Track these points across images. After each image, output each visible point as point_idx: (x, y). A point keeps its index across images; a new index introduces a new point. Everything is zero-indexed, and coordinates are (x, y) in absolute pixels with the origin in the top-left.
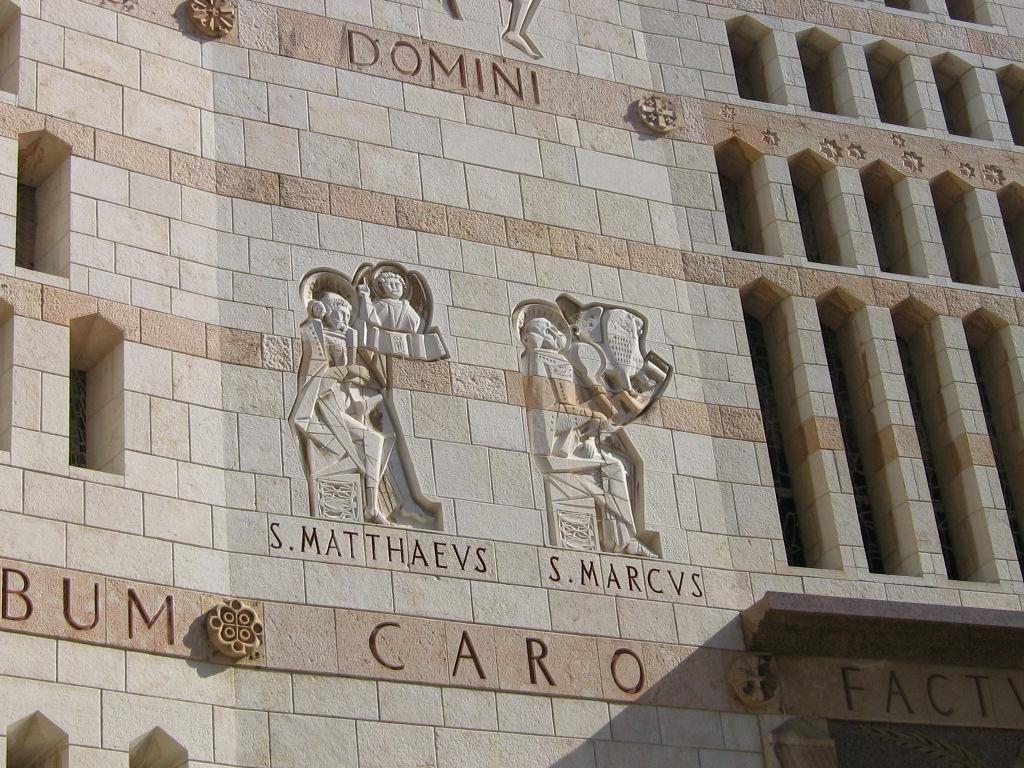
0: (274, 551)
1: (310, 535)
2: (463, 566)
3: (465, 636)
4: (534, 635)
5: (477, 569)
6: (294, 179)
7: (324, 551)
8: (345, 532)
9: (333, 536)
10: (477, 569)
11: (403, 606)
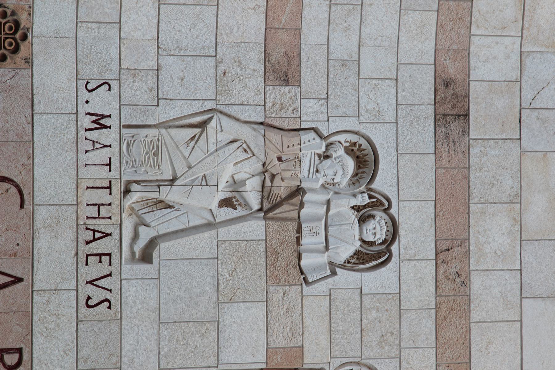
0: (82, 83)
1: (103, 122)
2: (91, 282)
3: (19, 280)
4: (25, 357)
5: (89, 298)
6: (466, 130)
7: (89, 134)
8: (110, 158)
9: (105, 146)
10: (89, 298)
11: (41, 215)
